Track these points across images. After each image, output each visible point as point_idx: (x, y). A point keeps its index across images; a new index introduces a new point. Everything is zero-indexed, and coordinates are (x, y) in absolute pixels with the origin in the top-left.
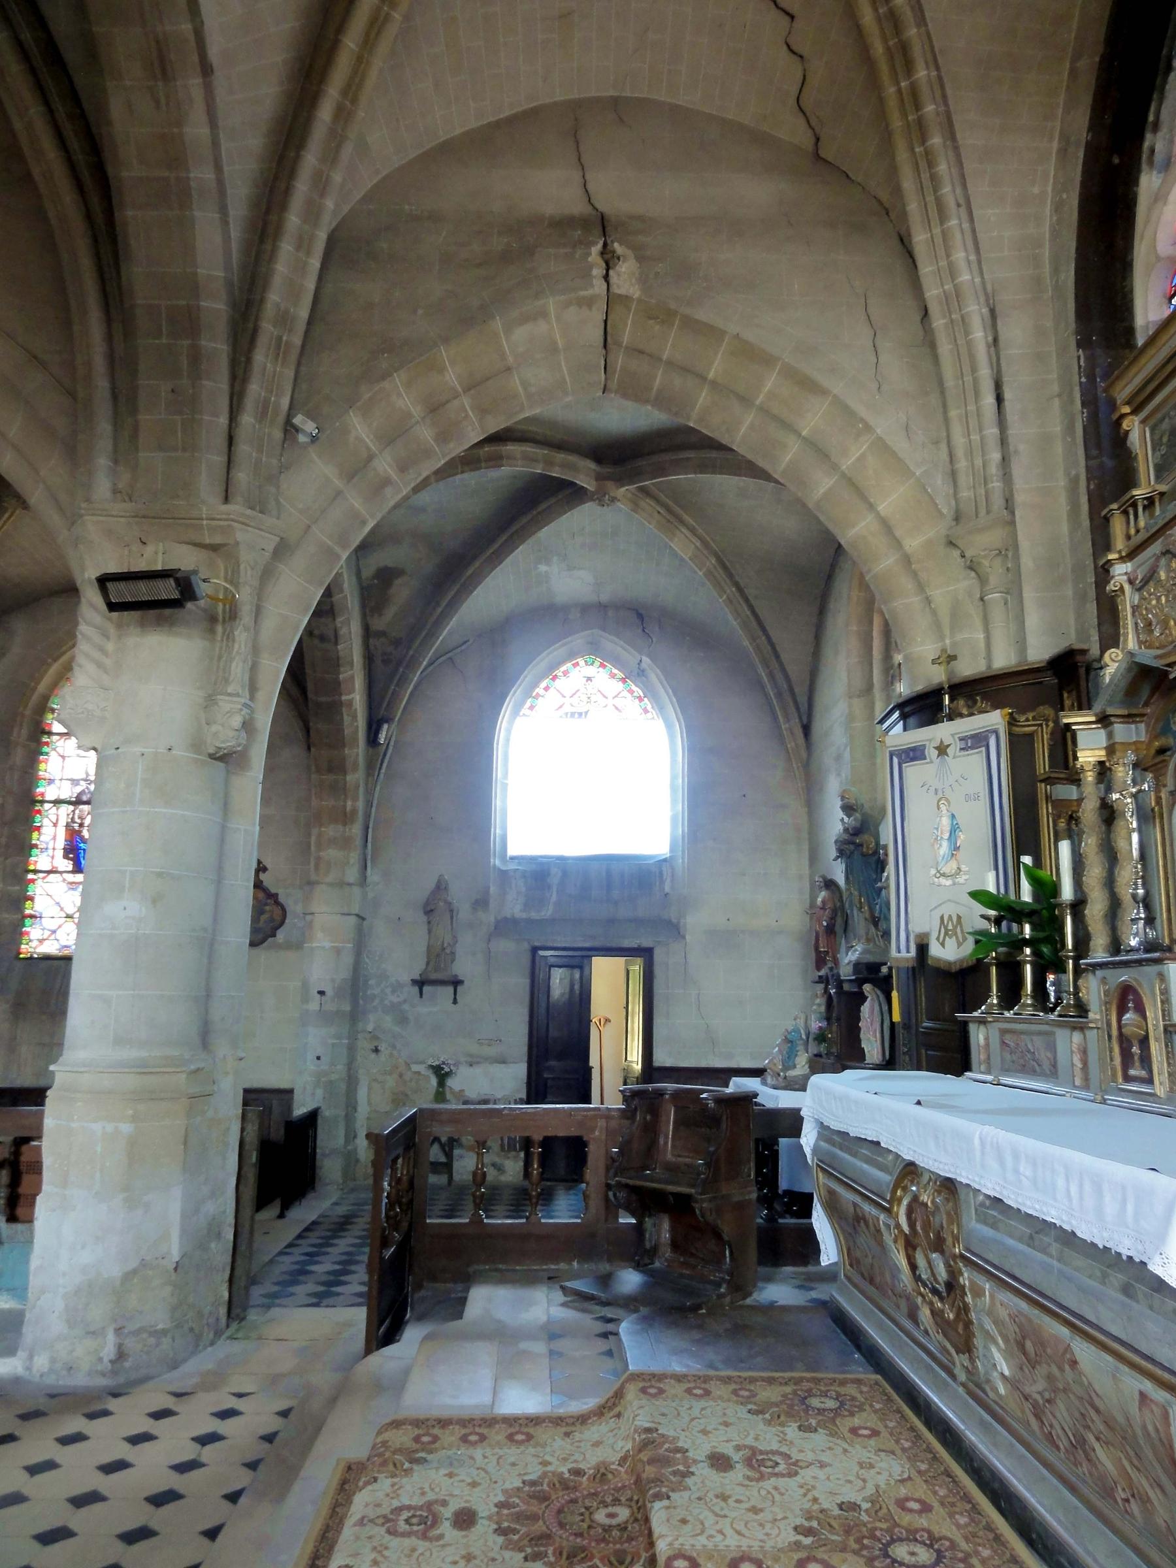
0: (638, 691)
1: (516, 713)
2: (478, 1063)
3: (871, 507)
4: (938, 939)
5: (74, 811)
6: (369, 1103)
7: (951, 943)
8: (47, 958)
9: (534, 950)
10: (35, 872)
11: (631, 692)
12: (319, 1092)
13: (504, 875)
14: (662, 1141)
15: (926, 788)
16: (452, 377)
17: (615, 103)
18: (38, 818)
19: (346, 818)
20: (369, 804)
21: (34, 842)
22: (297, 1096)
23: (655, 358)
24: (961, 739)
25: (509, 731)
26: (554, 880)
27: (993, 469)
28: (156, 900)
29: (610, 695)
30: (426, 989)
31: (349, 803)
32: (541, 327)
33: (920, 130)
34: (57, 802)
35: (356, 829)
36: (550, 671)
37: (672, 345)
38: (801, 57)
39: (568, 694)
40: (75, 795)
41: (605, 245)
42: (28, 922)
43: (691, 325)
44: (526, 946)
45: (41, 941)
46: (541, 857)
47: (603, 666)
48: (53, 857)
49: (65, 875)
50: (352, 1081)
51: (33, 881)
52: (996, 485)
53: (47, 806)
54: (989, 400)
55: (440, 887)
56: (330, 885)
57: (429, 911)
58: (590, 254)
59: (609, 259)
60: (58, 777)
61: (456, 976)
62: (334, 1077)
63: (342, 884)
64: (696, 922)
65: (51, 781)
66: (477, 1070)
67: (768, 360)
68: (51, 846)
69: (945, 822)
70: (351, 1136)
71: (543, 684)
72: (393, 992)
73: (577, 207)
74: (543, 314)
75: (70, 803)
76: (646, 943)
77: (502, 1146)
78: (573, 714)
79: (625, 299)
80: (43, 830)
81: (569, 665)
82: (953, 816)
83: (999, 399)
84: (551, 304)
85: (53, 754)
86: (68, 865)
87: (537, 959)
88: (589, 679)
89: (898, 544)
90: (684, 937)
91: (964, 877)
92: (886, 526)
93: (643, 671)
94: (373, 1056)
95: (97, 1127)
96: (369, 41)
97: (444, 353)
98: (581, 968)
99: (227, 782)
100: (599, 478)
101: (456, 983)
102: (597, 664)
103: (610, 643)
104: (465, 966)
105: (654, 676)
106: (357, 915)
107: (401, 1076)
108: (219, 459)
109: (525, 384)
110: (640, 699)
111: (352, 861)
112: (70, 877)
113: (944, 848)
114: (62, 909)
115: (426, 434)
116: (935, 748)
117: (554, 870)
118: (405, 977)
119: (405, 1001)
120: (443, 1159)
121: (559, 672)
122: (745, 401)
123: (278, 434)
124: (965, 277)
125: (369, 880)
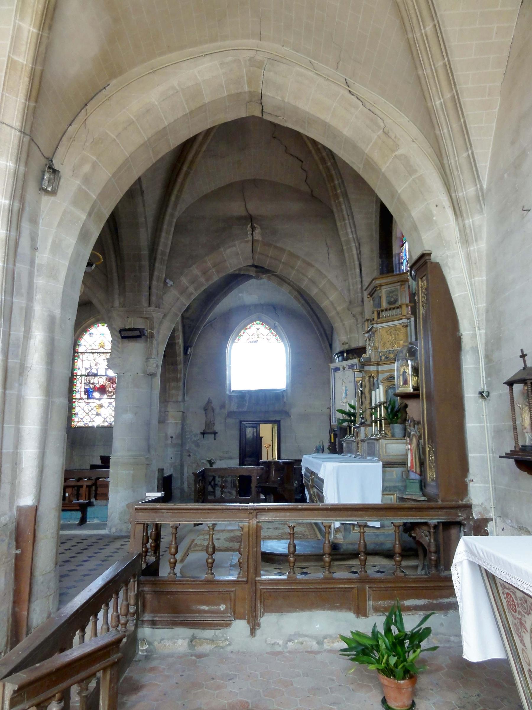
0: (275, 333)
1: (233, 341)
2: (223, 459)
3: (328, 298)
6: (188, 472)
8: (80, 427)
9: (241, 422)
10: (75, 399)
11: (272, 333)
12: (172, 469)
13: (230, 397)
14: (271, 475)
16: (209, 264)
17: (254, 180)
19: (177, 380)
20: (185, 375)
22: (165, 471)
23: (267, 256)
24: (348, 366)
25: (231, 348)
26: (247, 398)
27: (359, 290)
28: (136, 414)
29: (265, 335)
30: (205, 435)
31: (179, 375)
32: (234, 249)
33: (336, 196)
34: (81, 376)
35: (181, 384)
36: (244, 327)
37: (271, 252)
38: (306, 171)
39: (251, 335)
41: (252, 224)
42: (73, 416)
43: (276, 247)
44: (238, 421)
45: (78, 422)
46: (243, 390)
47: (262, 324)
48: (81, 394)
50: (182, 466)
51: (75, 402)
52: (360, 294)
53: (78, 377)
54: (358, 270)
55: (209, 402)
56: (173, 402)
57: (205, 410)
58: (247, 228)
59: (253, 229)
60: (81, 367)
61: (215, 431)
62: (177, 464)
63: (177, 402)
64: (294, 411)
65: (79, 369)
66: (222, 462)
67: (298, 257)
68: (80, 390)
69: (344, 388)
70: (182, 483)
71: (242, 331)
72: (195, 436)
73: (243, 213)
74: (235, 246)
75: (85, 376)
76: (278, 418)
77: (231, 486)
78: (252, 342)
79: (258, 241)
80: (77, 385)
81: (251, 324)
82: (346, 387)
83: (361, 270)
84: (237, 243)
85: (79, 359)
86: (85, 397)
87: (242, 425)
88: (258, 329)
89: (335, 308)
90: (291, 417)
92: (332, 303)
93: (276, 326)
94: (189, 457)
95: (124, 472)
96: (185, 179)
97: (207, 258)
98: (256, 427)
99: (151, 380)
100: (256, 272)
101: (215, 433)
102: (261, 324)
103: (265, 317)
104: (218, 427)
105: (280, 328)
106: (182, 412)
107: (198, 464)
108: (148, 294)
109: (230, 264)
110: (276, 336)
111: (180, 394)
112: (86, 401)
113: (344, 395)
114: (84, 411)
115: (202, 280)
117: (247, 395)
118: (199, 432)
119: (199, 440)
120: (212, 490)
121: (247, 327)
122: (293, 268)
123: (162, 285)
124: (351, 236)
125: (185, 400)
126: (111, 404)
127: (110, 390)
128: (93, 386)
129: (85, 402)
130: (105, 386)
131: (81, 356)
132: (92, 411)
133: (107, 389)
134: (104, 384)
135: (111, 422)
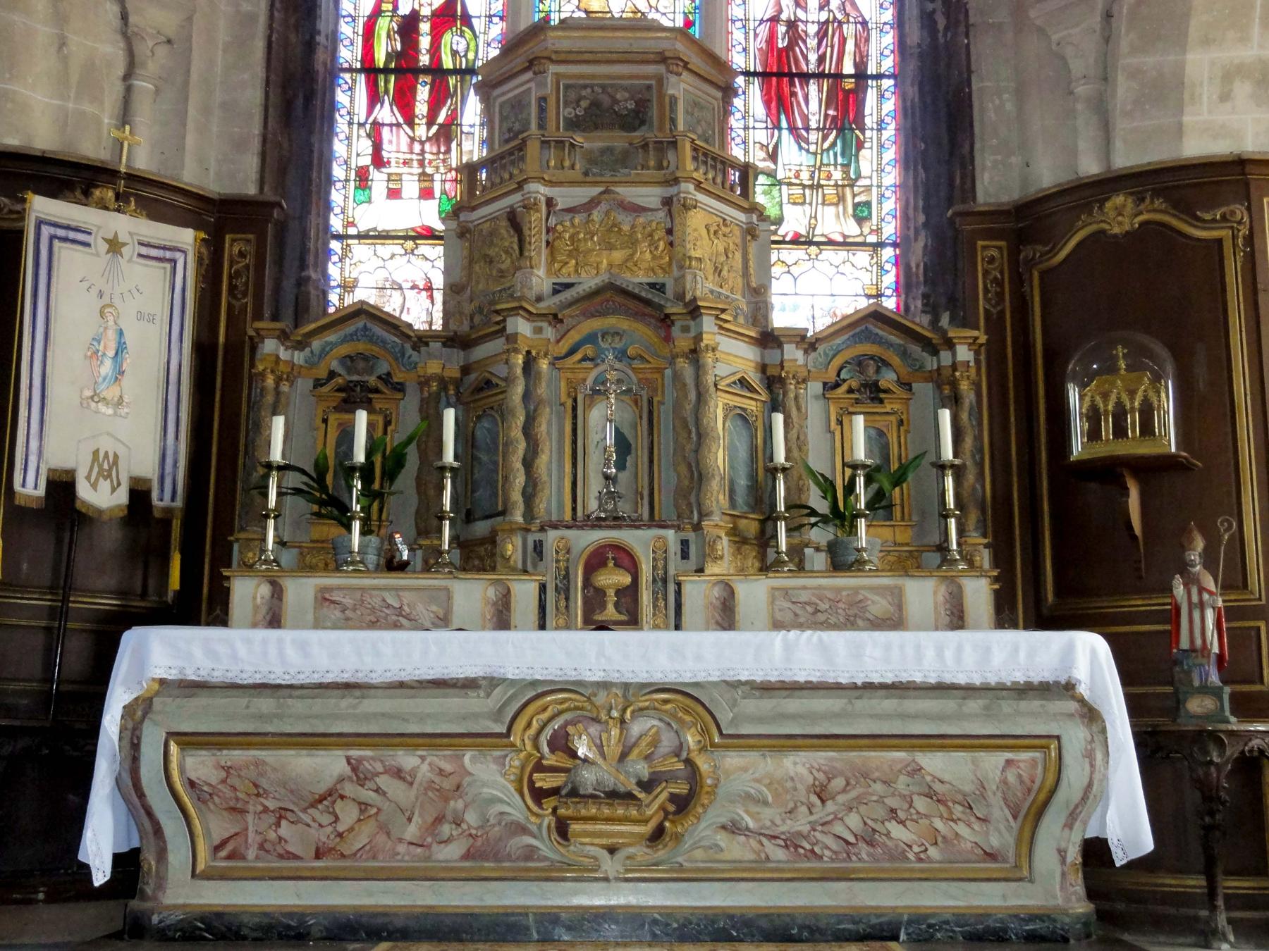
4: (88, 478)
7: (105, 485)
15: (86, 284)
91: (126, 410)
113: (107, 368)
116: (124, 244)
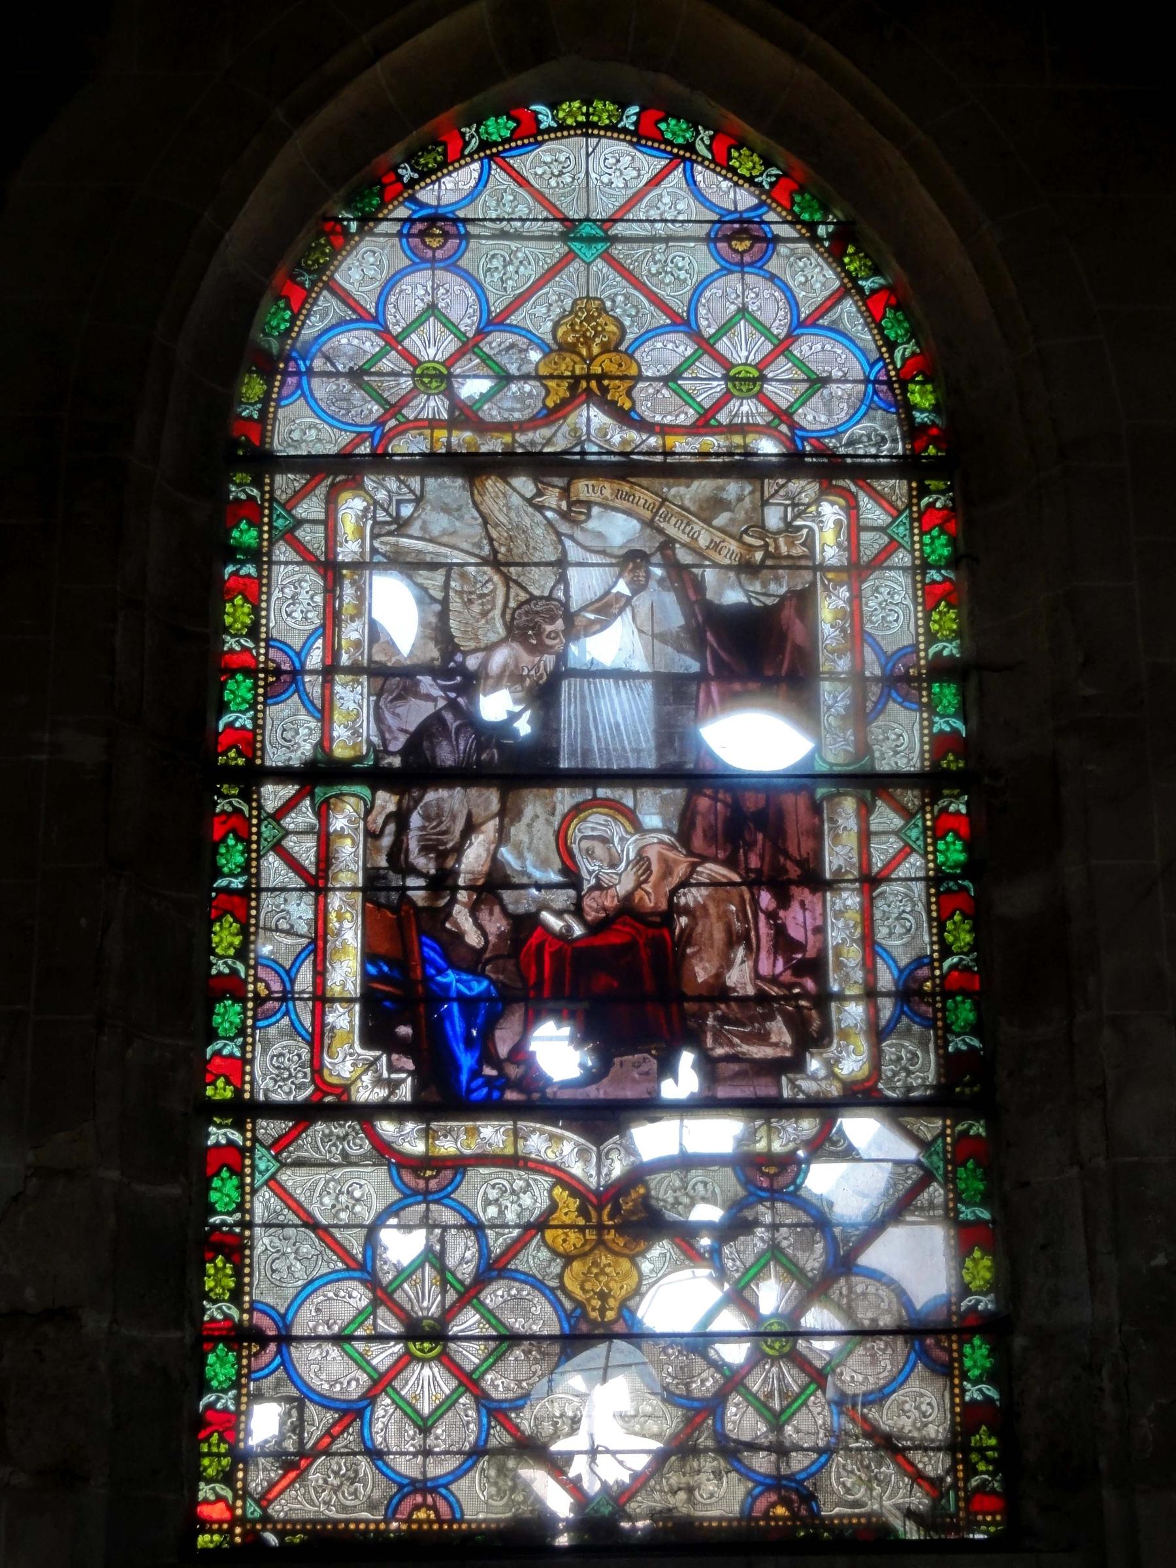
5: (400, 818)
18: (232, 856)
21: (220, 967)
40: (398, 743)
48: (318, 1039)
49: (386, 1128)
68: (304, 980)
85: (283, 551)
126: (774, 1194)
127: (739, 977)
128: (496, 924)
129: (383, 1150)
130: (673, 910)
131: (311, 508)
132: (495, 1295)
133: (702, 972)
134: (651, 899)
135: (798, 1462)
